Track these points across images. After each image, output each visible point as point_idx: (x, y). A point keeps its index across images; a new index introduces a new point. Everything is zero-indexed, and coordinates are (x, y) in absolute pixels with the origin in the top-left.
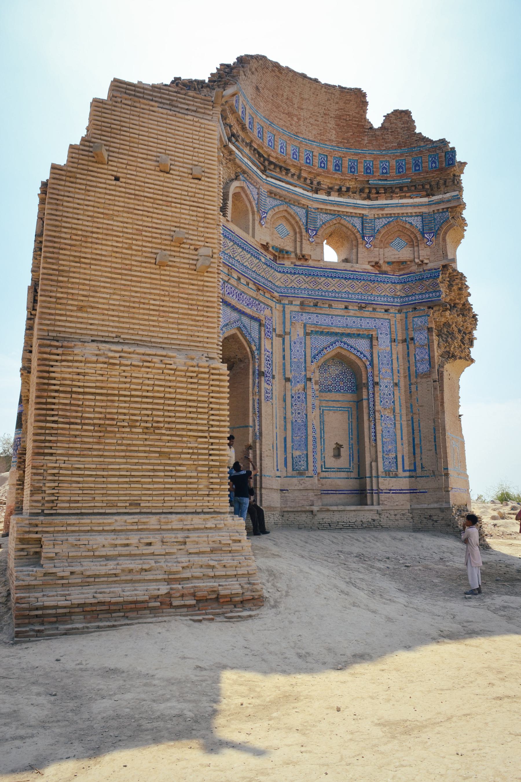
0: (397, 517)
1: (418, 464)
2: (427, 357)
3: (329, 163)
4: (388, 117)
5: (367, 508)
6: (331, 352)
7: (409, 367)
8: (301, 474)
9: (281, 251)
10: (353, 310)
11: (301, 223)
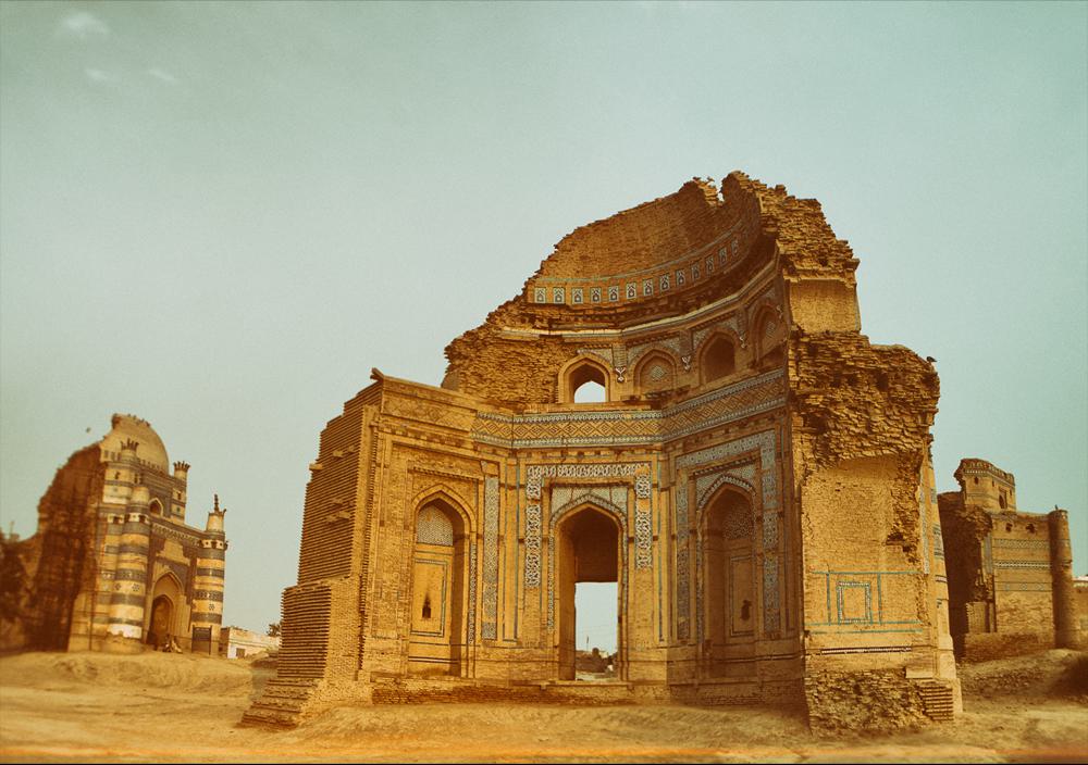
9: (659, 394)
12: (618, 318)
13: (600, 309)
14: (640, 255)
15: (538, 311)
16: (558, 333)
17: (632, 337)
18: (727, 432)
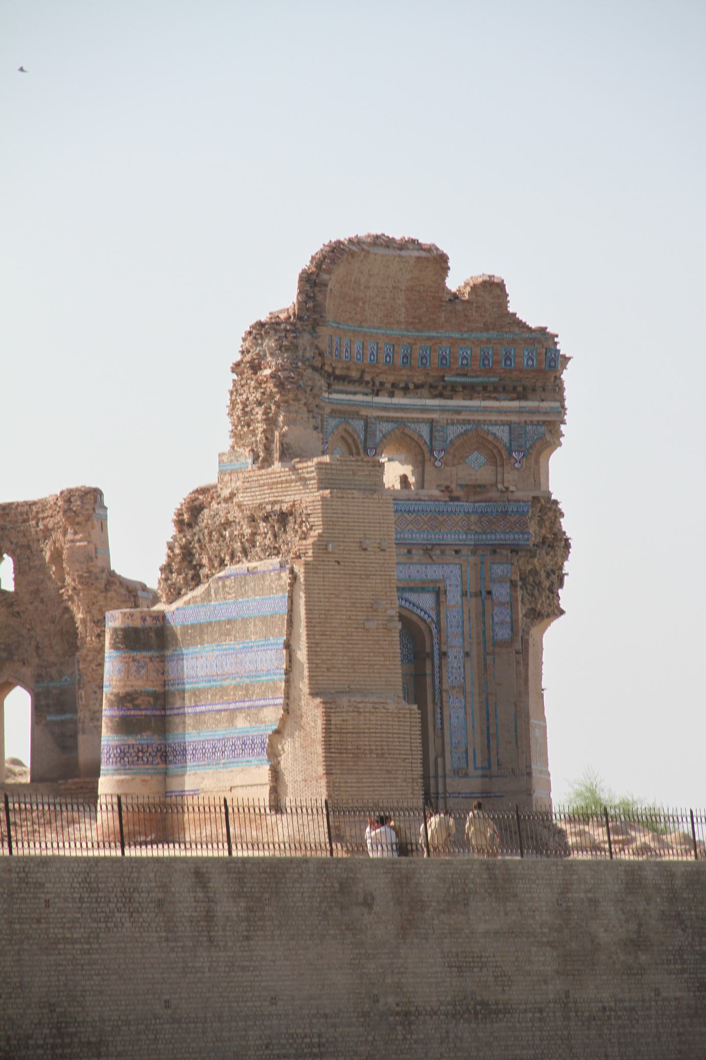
1: (494, 760)
2: (508, 620)
3: (396, 356)
7: (484, 632)
11: (359, 442)
18: (409, 552)
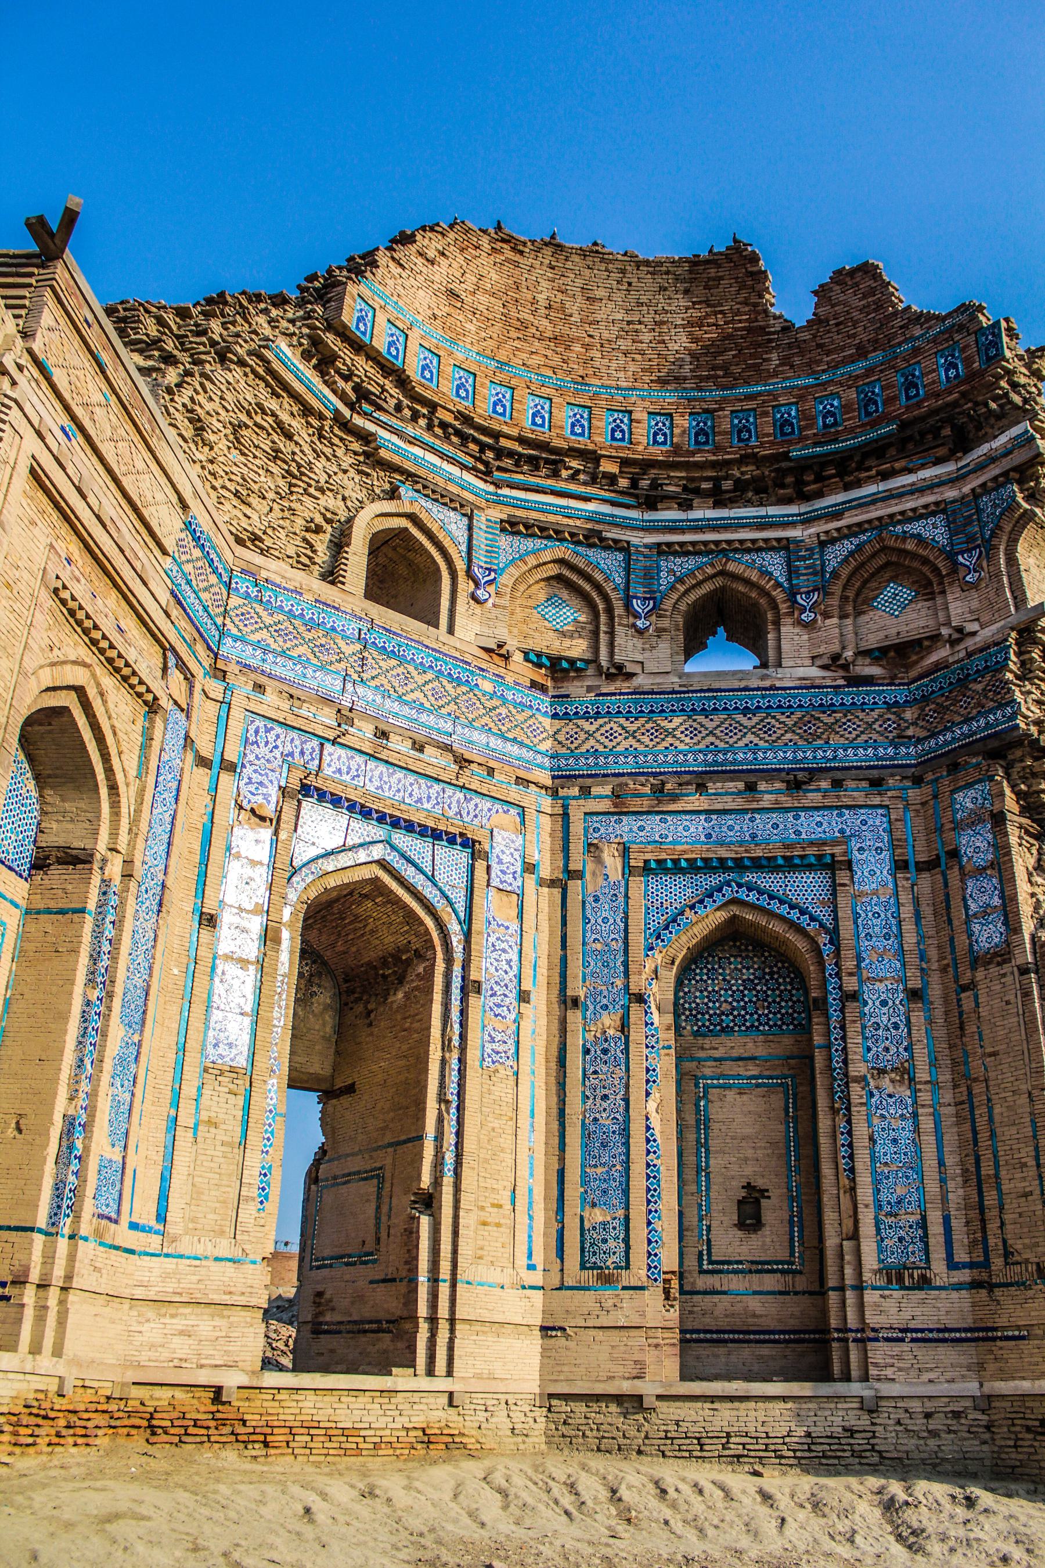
0: (934, 1424)
2: (996, 901)
4: (822, 293)
5: (826, 1389)
6: (711, 918)
7: (952, 940)
8: (607, 1280)
10: (769, 793)
11: (608, 588)
12: (498, 458)
13: (467, 420)
14: (568, 348)
15: (346, 354)
16: (371, 427)
17: (519, 513)
18: (751, 787)
